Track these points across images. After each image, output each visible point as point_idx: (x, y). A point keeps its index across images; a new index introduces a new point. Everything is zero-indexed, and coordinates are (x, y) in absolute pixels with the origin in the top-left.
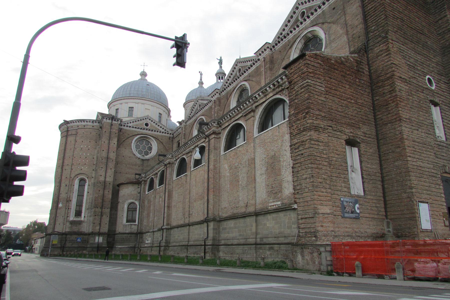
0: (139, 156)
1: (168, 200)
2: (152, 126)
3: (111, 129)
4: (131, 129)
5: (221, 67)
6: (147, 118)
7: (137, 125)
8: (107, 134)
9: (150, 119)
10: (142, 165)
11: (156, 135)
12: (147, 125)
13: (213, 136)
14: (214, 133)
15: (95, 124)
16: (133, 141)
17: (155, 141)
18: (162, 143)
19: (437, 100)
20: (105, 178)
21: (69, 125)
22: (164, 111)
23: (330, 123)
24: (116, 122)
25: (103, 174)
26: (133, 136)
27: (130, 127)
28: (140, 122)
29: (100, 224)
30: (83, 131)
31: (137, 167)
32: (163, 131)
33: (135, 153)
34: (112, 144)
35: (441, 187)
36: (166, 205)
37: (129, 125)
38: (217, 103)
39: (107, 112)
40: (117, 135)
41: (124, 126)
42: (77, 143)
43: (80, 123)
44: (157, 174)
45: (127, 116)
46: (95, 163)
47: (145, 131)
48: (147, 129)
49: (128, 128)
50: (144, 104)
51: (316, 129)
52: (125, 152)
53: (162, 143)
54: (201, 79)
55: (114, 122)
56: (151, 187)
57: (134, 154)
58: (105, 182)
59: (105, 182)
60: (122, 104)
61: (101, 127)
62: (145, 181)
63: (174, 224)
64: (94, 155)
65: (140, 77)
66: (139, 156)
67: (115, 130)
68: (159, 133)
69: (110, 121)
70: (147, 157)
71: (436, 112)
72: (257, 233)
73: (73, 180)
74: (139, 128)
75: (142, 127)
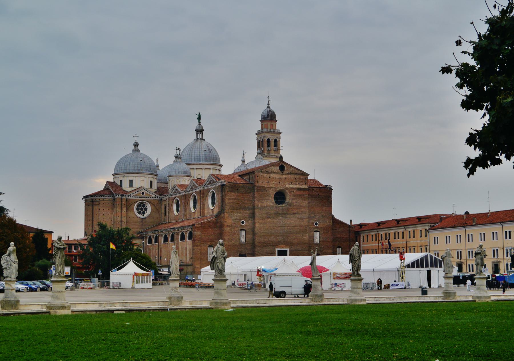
1: (160, 253)
2: (146, 194)
3: (121, 202)
4: (133, 198)
5: (200, 122)
7: (136, 195)
8: (120, 206)
9: (145, 190)
10: (142, 222)
11: (149, 200)
13: (176, 234)
14: (176, 233)
15: (110, 197)
16: (135, 206)
17: (149, 204)
18: (154, 205)
19: (244, 229)
21: (93, 198)
22: (154, 178)
23: (203, 242)
24: (124, 197)
27: (132, 197)
28: (139, 192)
30: (103, 202)
31: (138, 224)
32: (154, 196)
34: (123, 212)
36: (159, 255)
37: (132, 195)
38: (184, 197)
39: (112, 181)
40: (125, 205)
41: (129, 197)
42: (100, 211)
43: (101, 197)
44: (153, 236)
45: (129, 187)
46: (113, 223)
47: (142, 198)
48: (143, 197)
49: (131, 198)
50: (139, 177)
51: (197, 246)
52: (131, 214)
53: (154, 205)
55: (123, 197)
56: (150, 241)
57: (136, 215)
60: (124, 177)
61: (114, 199)
62: (146, 237)
63: (163, 264)
64: (112, 218)
67: (124, 202)
68: (151, 199)
70: (145, 216)
71: (243, 233)
72: (187, 271)
74: (138, 197)
75: (140, 196)
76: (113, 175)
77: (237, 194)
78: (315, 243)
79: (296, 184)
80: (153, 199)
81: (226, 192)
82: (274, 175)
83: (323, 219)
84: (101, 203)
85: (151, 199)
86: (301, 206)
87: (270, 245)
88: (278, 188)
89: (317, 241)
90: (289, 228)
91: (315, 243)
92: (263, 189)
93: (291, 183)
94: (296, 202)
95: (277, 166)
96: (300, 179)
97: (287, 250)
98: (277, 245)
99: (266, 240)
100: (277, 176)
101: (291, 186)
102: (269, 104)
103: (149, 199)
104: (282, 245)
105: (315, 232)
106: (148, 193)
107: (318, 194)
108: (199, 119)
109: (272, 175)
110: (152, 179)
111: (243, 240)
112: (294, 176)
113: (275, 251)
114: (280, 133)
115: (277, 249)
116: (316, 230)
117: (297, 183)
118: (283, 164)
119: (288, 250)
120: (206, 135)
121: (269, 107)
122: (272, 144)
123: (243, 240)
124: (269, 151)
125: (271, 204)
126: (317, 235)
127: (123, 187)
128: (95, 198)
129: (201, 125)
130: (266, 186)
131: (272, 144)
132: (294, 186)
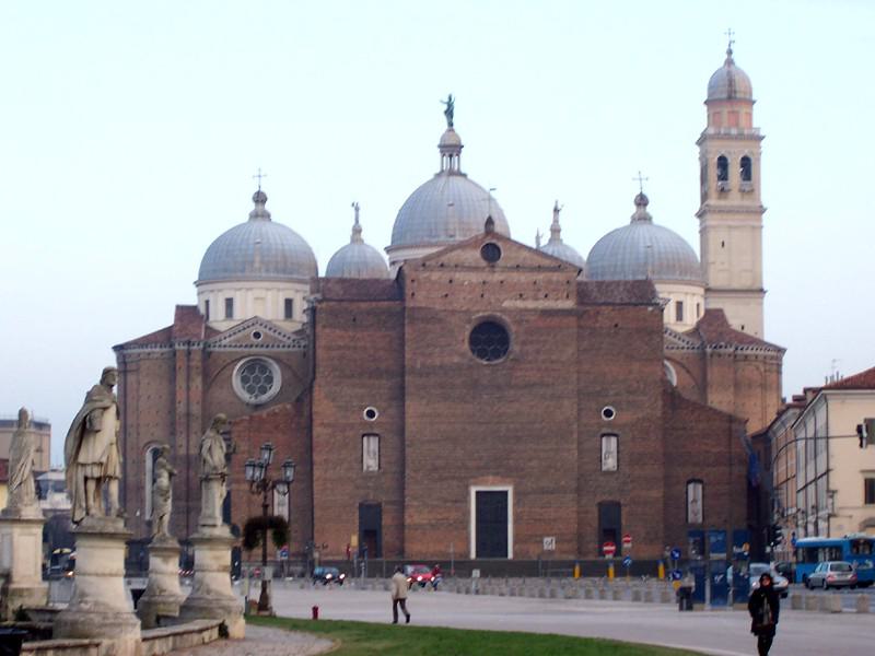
0: (246, 396)
2: (266, 335)
3: (189, 360)
4: (228, 349)
5: (451, 124)
6: (256, 321)
7: (238, 341)
12: (257, 335)
15: (164, 350)
16: (235, 372)
19: (376, 431)
20: (188, 449)
25: (184, 443)
26: (233, 362)
29: (188, 527)
33: (239, 394)
34: (193, 388)
35: (357, 514)
37: (224, 342)
42: (142, 385)
47: (254, 350)
48: (257, 346)
49: (222, 349)
52: (218, 394)
54: (357, 221)
57: (237, 397)
58: (188, 456)
59: (188, 456)
65: (252, 206)
66: (246, 396)
67: (197, 360)
69: (186, 347)
70: (264, 398)
71: (371, 445)
73: (142, 453)
74: (241, 346)
76: (198, 284)
77: (351, 333)
78: (604, 468)
79: (536, 299)
80: (286, 349)
81: (319, 328)
82: (463, 274)
83: (631, 398)
84: (144, 365)
85: (281, 349)
86: (552, 362)
87: (453, 478)
88: (478, 311)
89: (610, 463)
90: (512, 426)
91: (604, 468)
92: (431, 317)
93: (521, 295)
94: (538, 352)
95: (475, 247)
96: (550, 282)
97: (506, 493)
98: (472, 477)
99: (439, 463)
100: (475, 278)
101: (520, 304)
102: (730, 52)
103: (275, 349)
104: (491, 478)
105: (604, 439)
106: (271, 333)
107: (616, 325)
108: (449, 113)
109: (458, 276)
110: (290, 295)
111: (371, 463)
112: (528, 274)
113: (468, 494)
114: (761, 138)
115: (473, 490)
116: (604, 430)
117: (541, 295)
118: (494, 241)
119: (510, 490)
120: (466, 162)
121: (730, 62)
122: (735, 170)
123: (371, 463)
124: (723, 192)
125: (456, 359)
126: (609, 445)
127: (211, 319)
128: (129, 351)
129: (453, 130)
130: (438, 307)
131: (735, 170)
132: (530, 304)
